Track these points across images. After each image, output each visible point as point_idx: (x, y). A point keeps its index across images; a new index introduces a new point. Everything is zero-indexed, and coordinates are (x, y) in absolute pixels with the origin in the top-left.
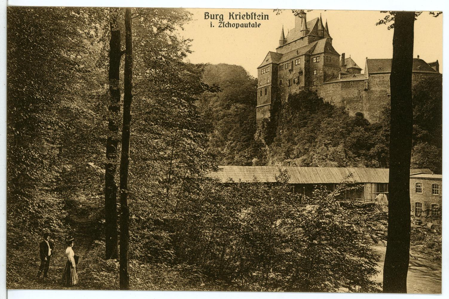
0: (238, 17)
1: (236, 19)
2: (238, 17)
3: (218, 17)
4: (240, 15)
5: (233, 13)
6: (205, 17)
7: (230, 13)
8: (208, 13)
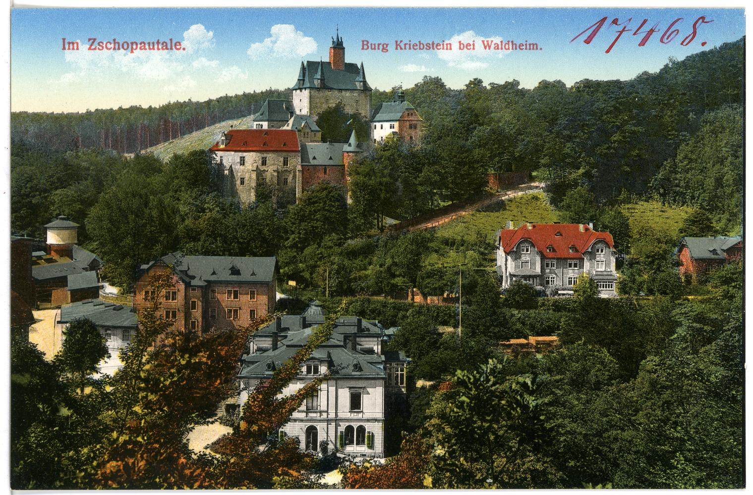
0: (407, 46)
1: (405, 49)
2: (407, 46)
3: (381, 47)
4: (410, 45)
5: (401, 41)
6: (363, 46)
7: (396, 42)
8: (368, 42)
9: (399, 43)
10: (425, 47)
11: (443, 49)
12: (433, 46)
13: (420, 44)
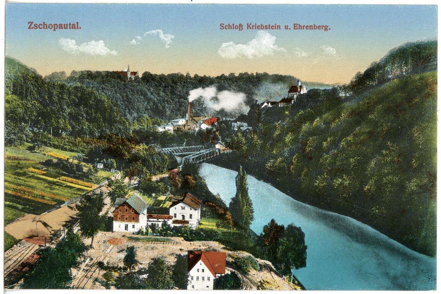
0: (254, 27)
1: (253, 29)
2: (254, 27)
4: (256, 26)
5: (250, 24)
7: (248, 24)
9: (249, 25)
10: (265, 27)
11: (275, 29)
12: (269, 27)
13: (314, 26)
